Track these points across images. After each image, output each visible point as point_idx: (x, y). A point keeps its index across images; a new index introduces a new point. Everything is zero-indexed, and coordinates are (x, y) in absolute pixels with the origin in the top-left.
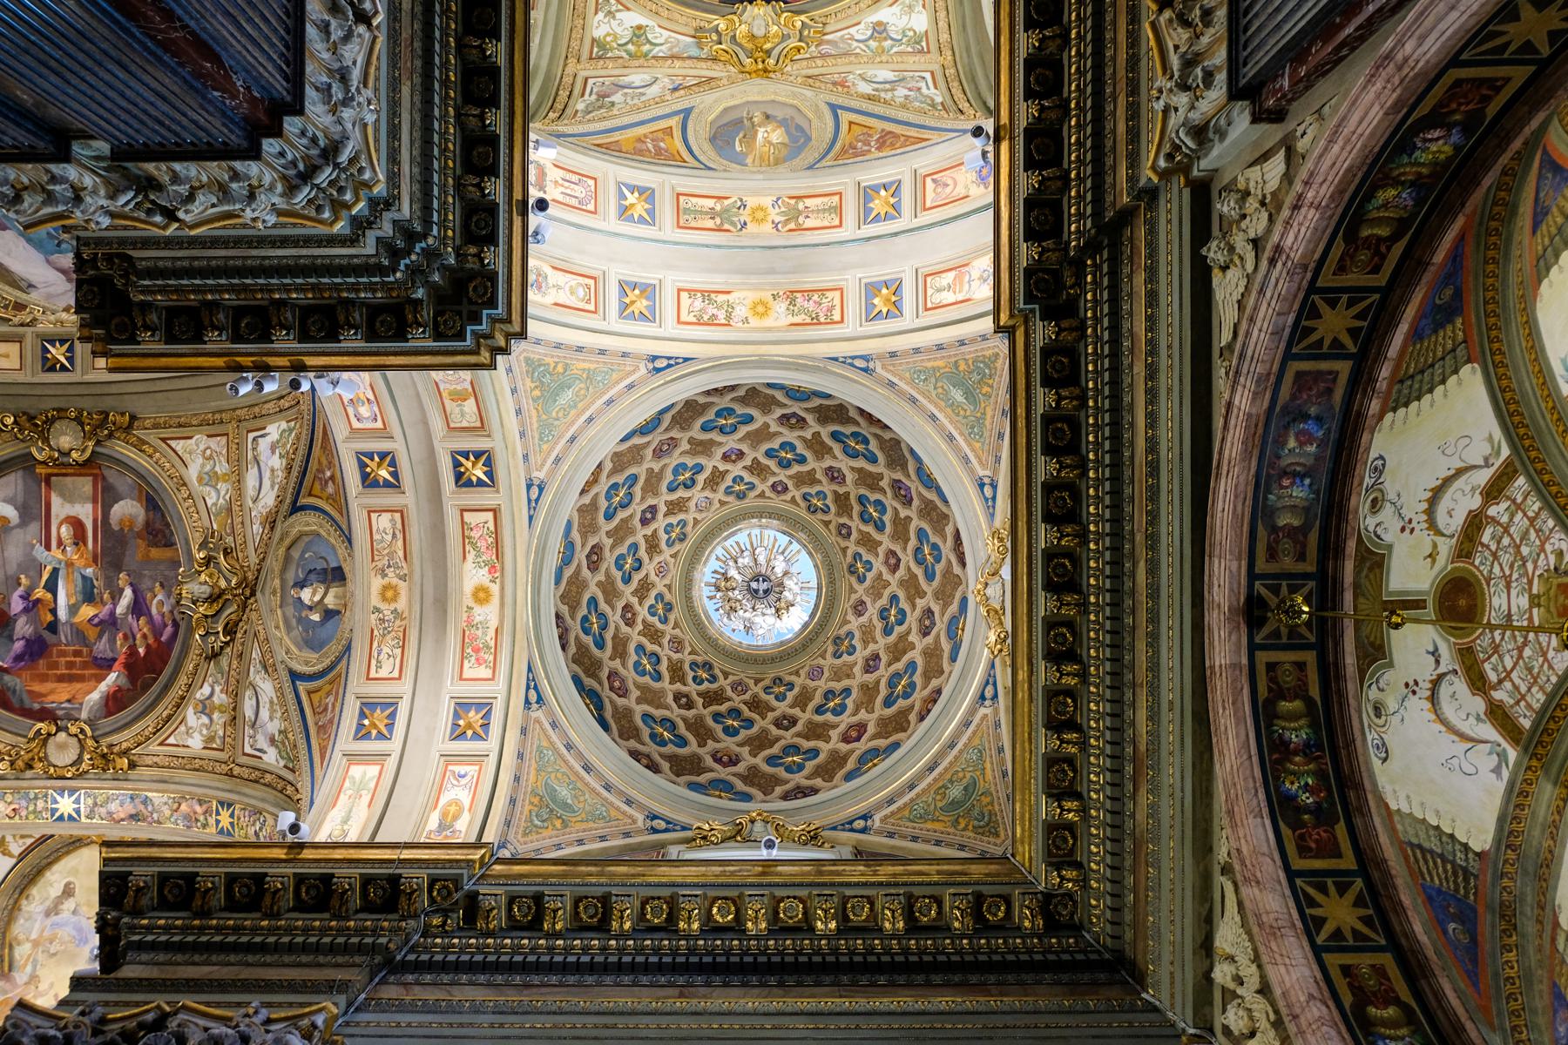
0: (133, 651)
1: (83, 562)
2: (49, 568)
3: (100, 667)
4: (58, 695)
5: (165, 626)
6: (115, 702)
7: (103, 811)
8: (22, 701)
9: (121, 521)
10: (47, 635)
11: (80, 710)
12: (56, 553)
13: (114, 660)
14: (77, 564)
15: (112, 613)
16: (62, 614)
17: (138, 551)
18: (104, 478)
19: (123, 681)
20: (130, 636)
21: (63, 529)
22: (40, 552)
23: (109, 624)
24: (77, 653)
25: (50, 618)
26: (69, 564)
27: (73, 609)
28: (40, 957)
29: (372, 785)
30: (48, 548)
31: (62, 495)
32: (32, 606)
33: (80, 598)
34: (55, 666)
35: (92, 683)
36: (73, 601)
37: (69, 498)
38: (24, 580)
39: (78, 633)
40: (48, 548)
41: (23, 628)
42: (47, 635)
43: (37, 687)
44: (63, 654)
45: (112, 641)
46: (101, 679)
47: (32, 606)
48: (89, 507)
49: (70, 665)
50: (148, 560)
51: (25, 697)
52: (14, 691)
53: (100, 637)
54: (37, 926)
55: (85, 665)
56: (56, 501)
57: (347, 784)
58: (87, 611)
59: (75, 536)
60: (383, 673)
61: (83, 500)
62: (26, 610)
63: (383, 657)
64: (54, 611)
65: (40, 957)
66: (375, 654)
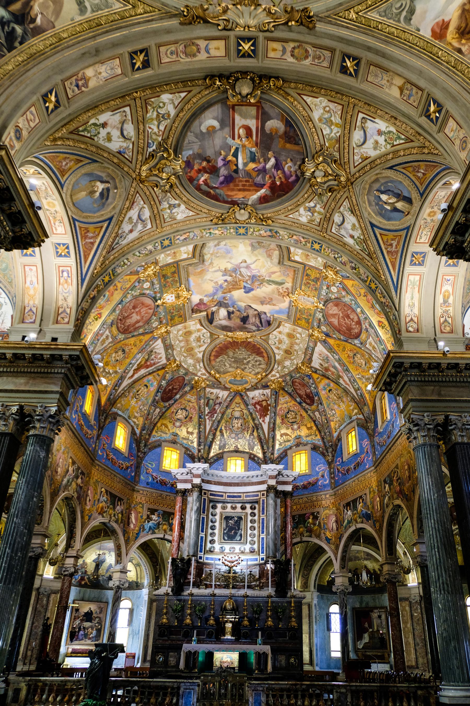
0: (274, 183)
1: (250, 145)
2: (234, 147)
3: (257, 187)
4: (239, 196)
5: (291, 176)
6: (264, 200)
7: (257, 233)
8: (224, 198)
9: (271, 130)
10: (234, 174)
11: (248, 201)
12: (237, 141)
13: (264, 185)
14: (248, 146)
15: (264, 167)
16: (240, 166)
17: (279, 144)
18: (262, 108)
19: (268, 193)
20: (273, 177)
21: (241, 131)
22: (230, 141)
23: (263, 171)
24: (247, 181)
25: (235, 167)
26: (244, 146)
27: (245, 164)
28: (213, 258)
29: (418, 283)
30: (234, 139)
31: (241, 115)
32: (227, 163)
33: (249, 160)
34: (238, 185)
35: (254, 192)
36: (245, 161)
37: (244, 116)
38: (223, 152)
39: (248, 174)
40: (234, 139)
41: (223, 172)
42: (234, 174)
43: (229, 193)
44: (241, 181)
45: (264, 178)
46: (257, 191)
47: (227, 163)
48: (254, 121)
49: (244, 185)
50: (284, 148)
51: (225, 197)
52: (221, 195)
53: (258, 175)
54: (212, 249)
55: (251, 186)
56: (237, 117)
57: (409, 283)
58: (252, 166)
59: (247, 134)
60: (422, 241)
61: (252, 118)
62: (224, 165)
63: (423, 235)
64: (237, 165)
65: (213, 258)
66: (420, 234)
